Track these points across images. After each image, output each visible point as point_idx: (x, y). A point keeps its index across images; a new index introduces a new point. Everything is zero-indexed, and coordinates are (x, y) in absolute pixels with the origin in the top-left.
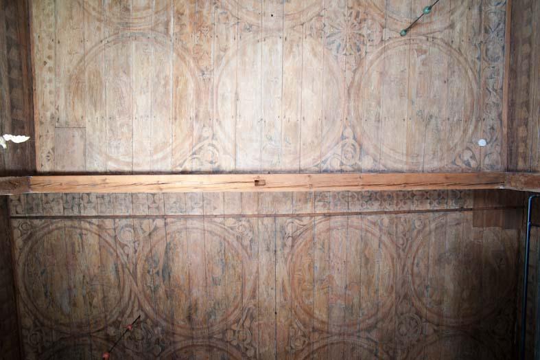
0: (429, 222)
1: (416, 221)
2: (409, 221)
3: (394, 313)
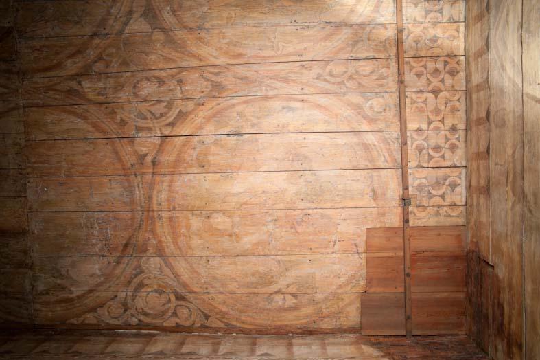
0: (381, 131)
1: (381, 100)
2: (382, 85)
3: (184, 64)
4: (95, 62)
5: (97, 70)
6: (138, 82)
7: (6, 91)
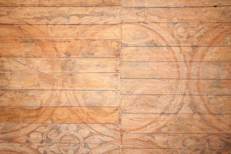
4: (162, 128)
5: (163, 132)
6: (185, 139)
7: (113, 140)
